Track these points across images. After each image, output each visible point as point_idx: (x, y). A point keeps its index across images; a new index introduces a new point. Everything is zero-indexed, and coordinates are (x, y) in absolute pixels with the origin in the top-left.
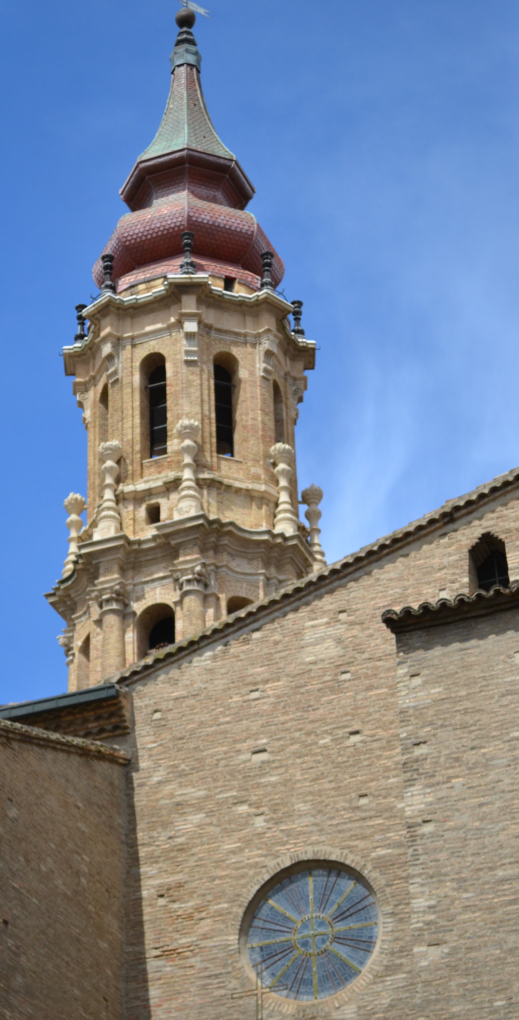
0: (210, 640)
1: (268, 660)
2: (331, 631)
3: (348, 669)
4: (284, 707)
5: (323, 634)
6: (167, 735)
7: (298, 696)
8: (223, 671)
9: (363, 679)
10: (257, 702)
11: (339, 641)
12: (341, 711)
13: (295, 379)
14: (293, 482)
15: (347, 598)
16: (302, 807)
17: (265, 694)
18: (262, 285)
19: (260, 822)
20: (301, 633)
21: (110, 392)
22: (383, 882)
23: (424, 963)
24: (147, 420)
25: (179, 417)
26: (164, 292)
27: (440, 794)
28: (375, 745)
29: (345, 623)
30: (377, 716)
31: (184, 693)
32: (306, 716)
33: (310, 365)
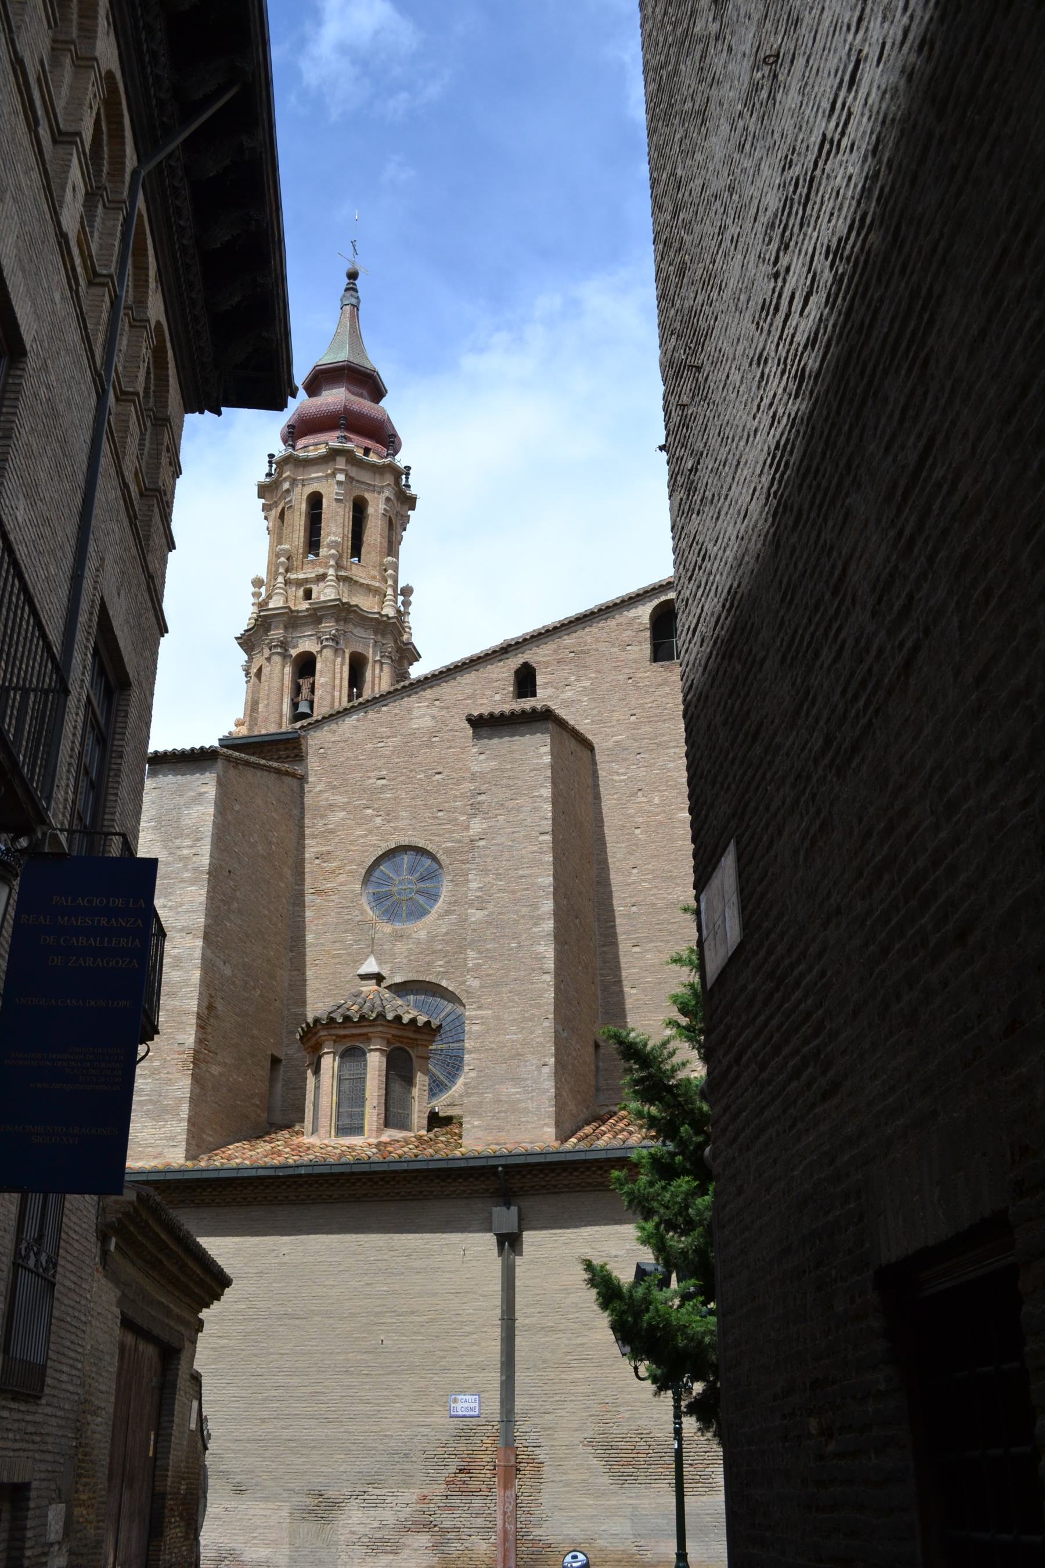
1: (391, 724)
2: (429, 711)
6: (326, 763)
8: (363, 728)
11: (434, 717)
14: (396, 582)
16: (404, 814)
18: (388, 455)
19: (378, 820)
21: (286, 513)
22: (448, 862)
23: (473, 919)
24: (308, 533)
25: (328, 535)
27: (491, 824)
28: (450, 781)
30: (452, 764)
31: (339, 739)
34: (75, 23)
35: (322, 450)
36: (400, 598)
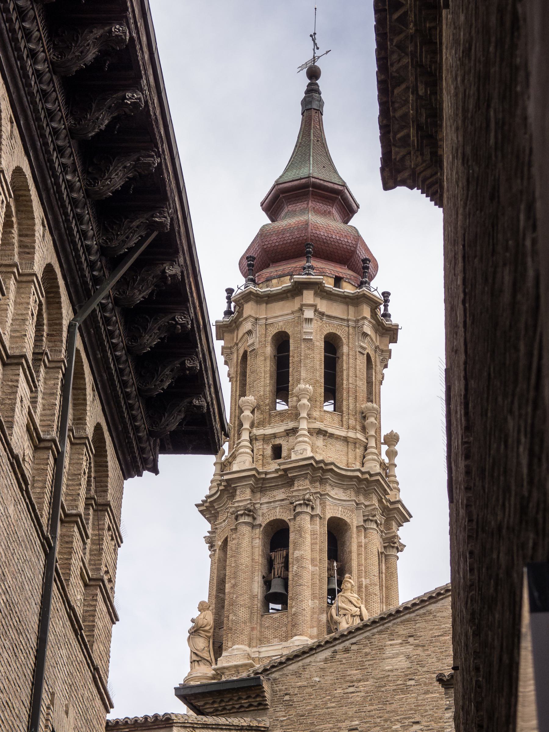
0: (323, 648)
1: (361, 666)
2: (403, 649)
3: (413, 677)
4: (371, 700)
5: (397, 651)
6: (293, 712)
7: (380, 693)
8: (331, 670)
9: (423, 685)
10: (353, 695)
11: (408, 657)
12: (407, 707)
13: (382, 351)
14: (378, 430)
15: (414, 627)
17: (358, 690)
20: (383, 649)
21: (249, 358)
24: (274, 380)
26: (290, 287)
29: (412, 645)
31: (305, 683)
32: (384, 708)
33: (394, 339)
34: (16, 244)
35: (287, 283)
36: (384, 448)
